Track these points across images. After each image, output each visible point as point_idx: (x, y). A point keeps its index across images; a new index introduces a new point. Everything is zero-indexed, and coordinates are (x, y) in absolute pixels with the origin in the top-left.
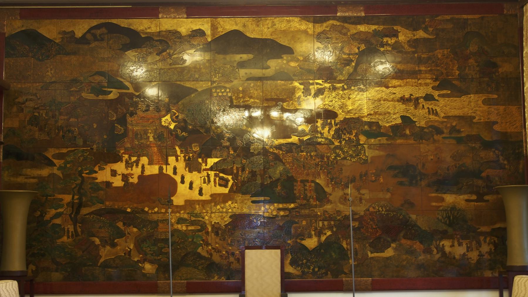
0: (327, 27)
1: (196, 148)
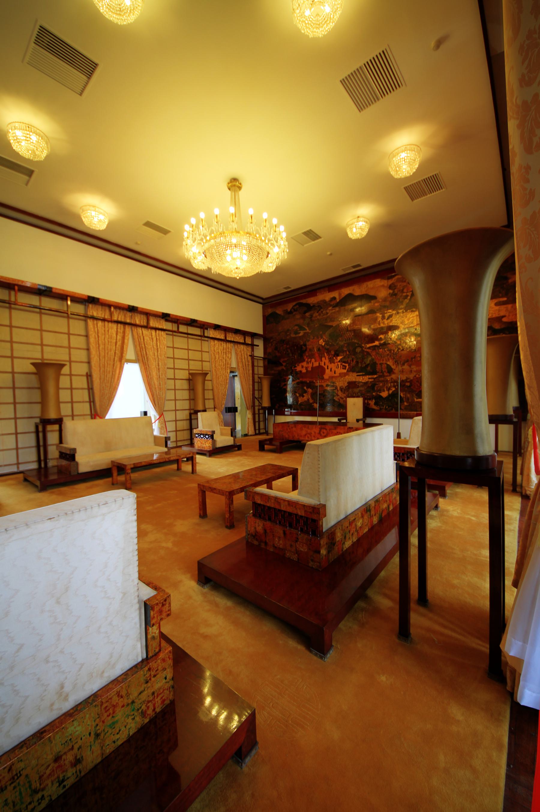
1: (333, 353)
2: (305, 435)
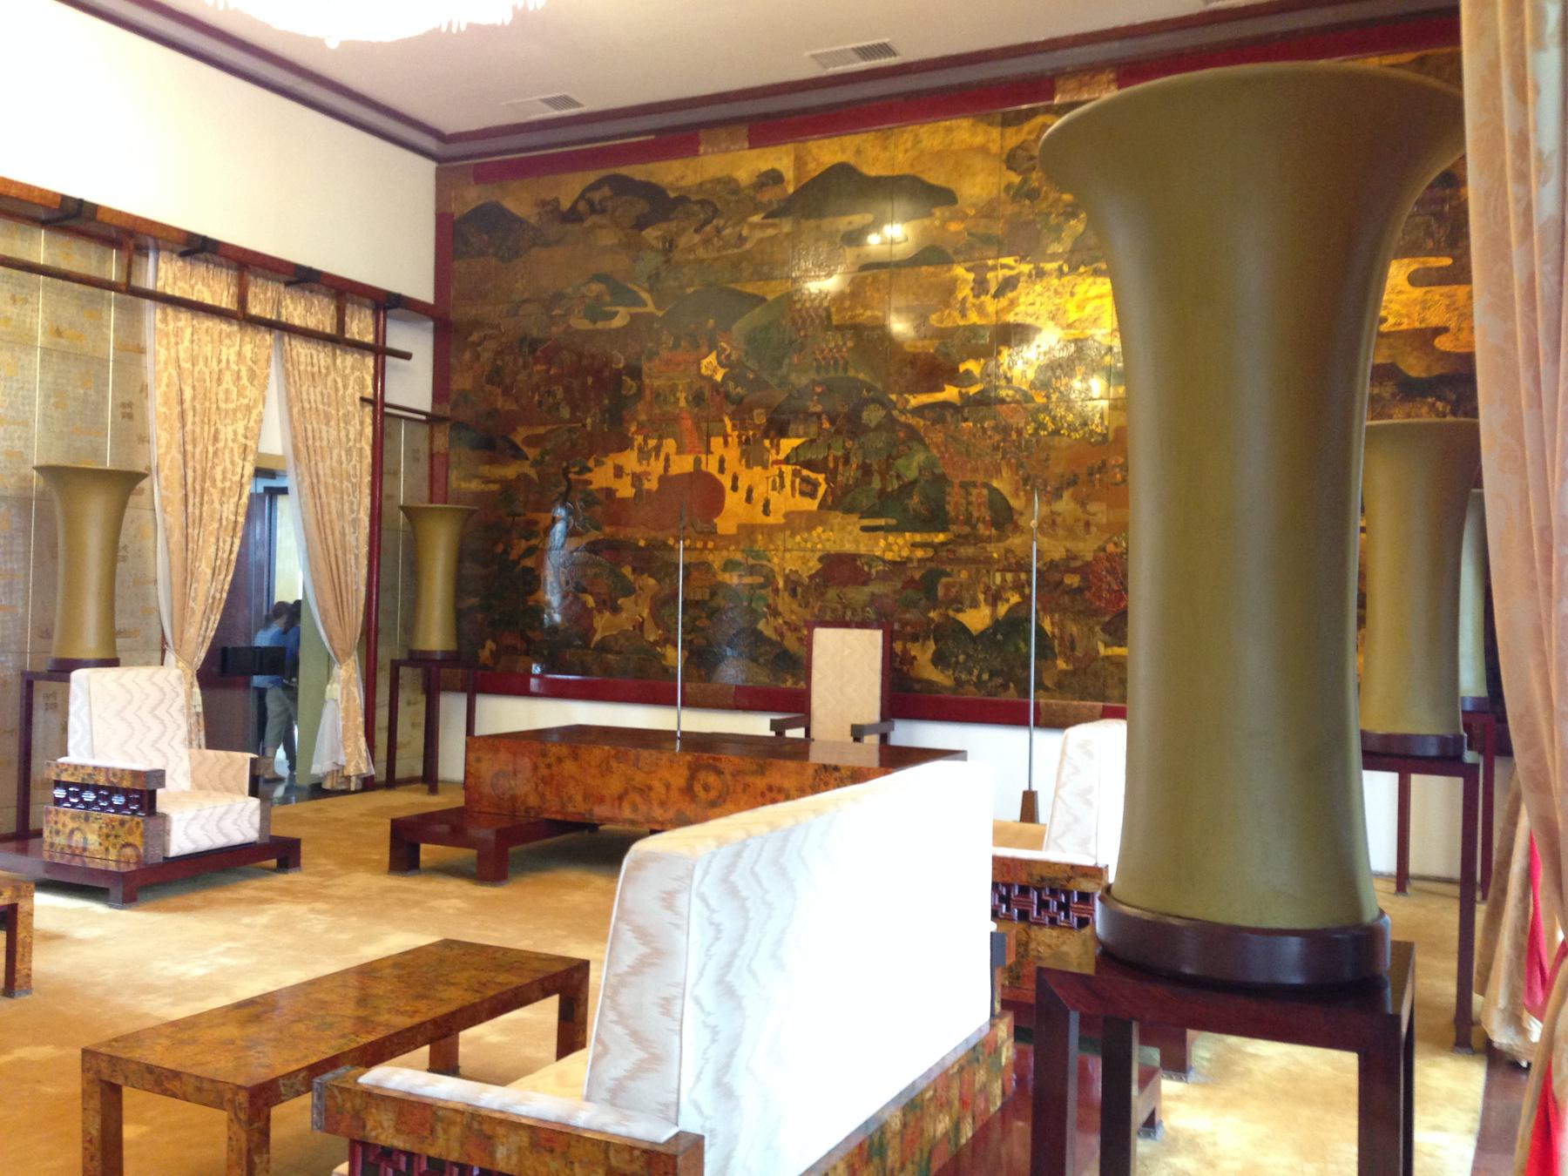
0: (1030, 133)
1: (760, 417)
2: (621, 798)
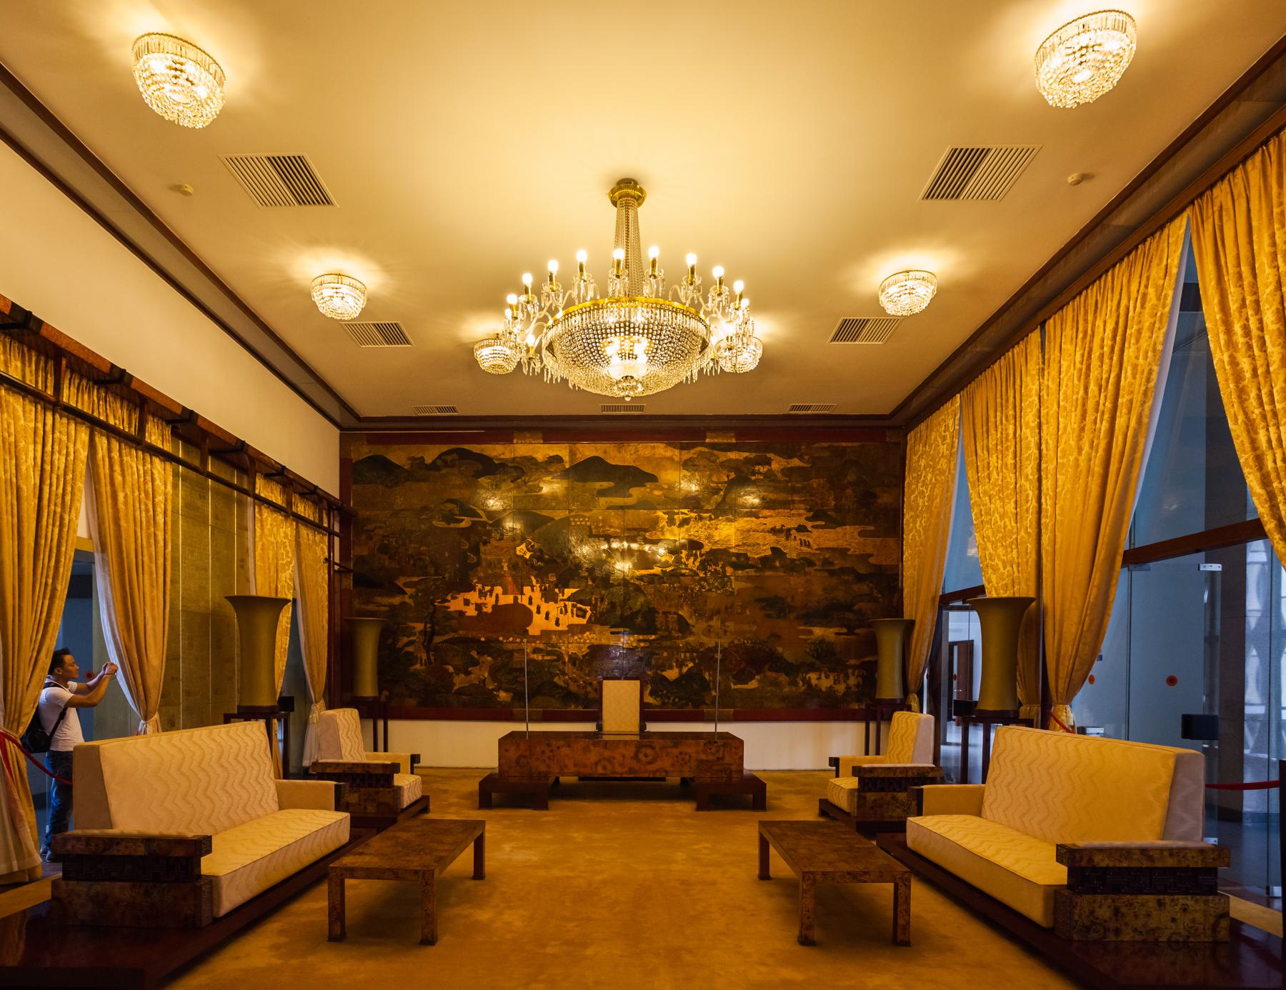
1: (553, 578)
